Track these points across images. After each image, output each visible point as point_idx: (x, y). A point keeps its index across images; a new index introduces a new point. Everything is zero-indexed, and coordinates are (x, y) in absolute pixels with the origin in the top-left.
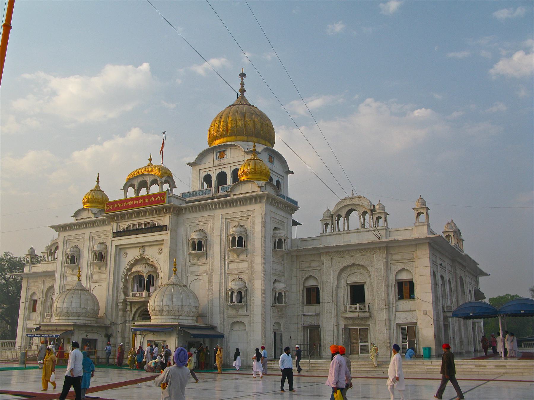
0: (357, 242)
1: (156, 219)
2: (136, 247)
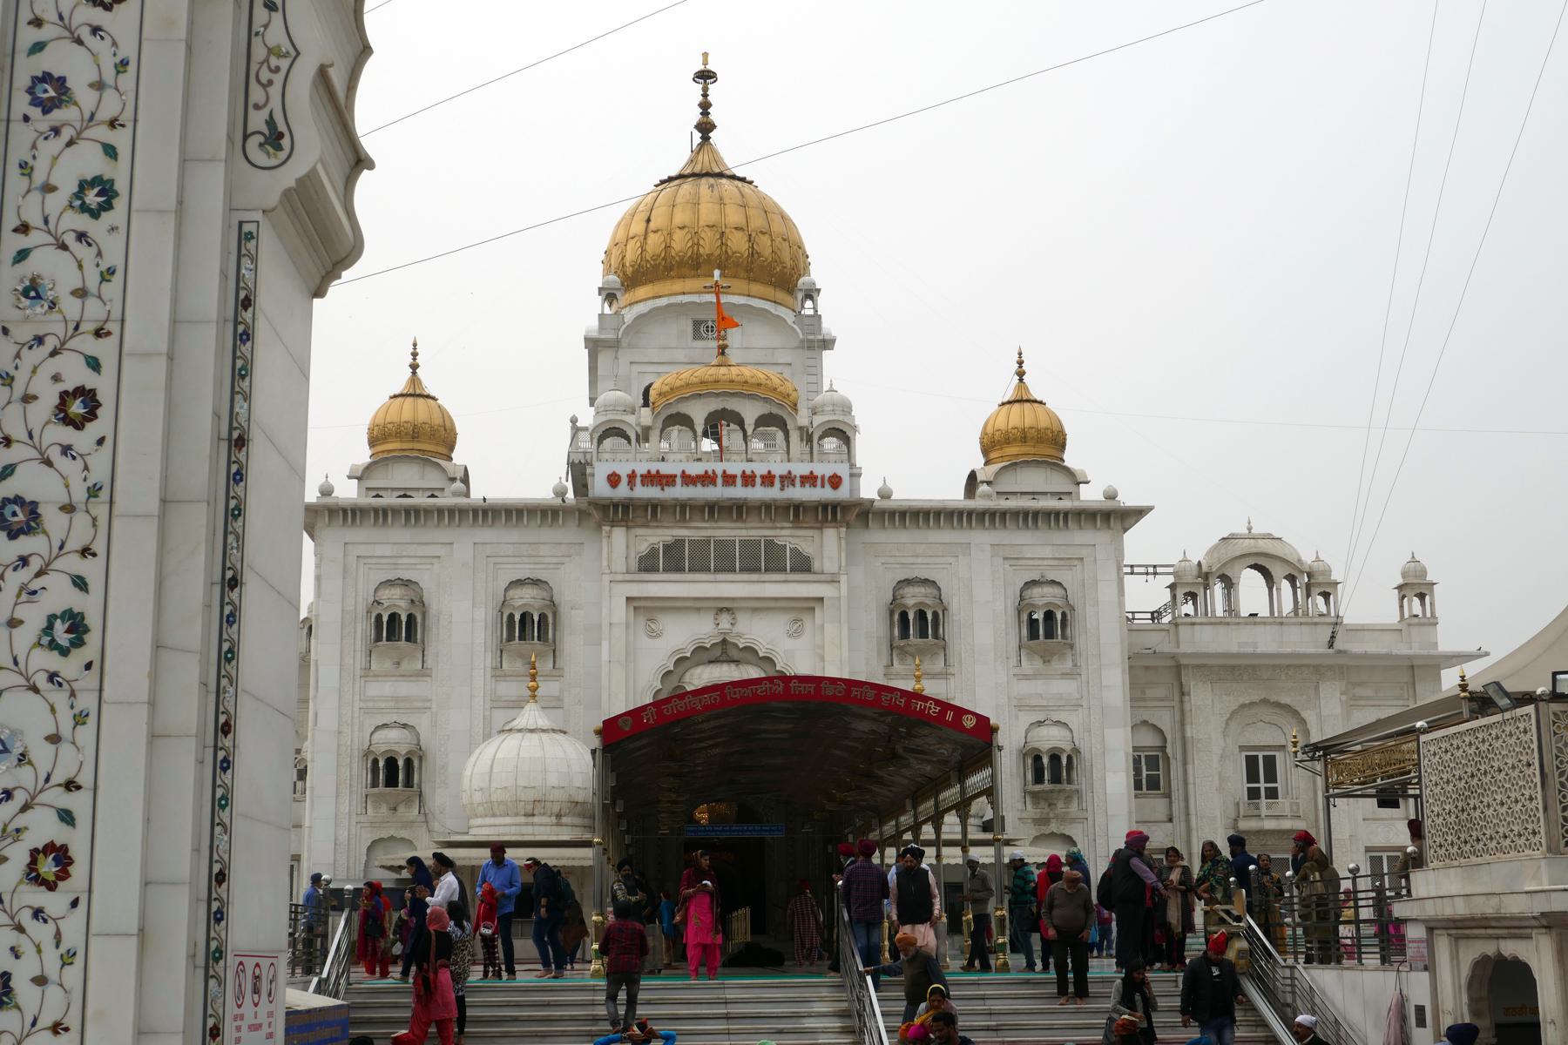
0: (1272, 648)
2: (699, 609)
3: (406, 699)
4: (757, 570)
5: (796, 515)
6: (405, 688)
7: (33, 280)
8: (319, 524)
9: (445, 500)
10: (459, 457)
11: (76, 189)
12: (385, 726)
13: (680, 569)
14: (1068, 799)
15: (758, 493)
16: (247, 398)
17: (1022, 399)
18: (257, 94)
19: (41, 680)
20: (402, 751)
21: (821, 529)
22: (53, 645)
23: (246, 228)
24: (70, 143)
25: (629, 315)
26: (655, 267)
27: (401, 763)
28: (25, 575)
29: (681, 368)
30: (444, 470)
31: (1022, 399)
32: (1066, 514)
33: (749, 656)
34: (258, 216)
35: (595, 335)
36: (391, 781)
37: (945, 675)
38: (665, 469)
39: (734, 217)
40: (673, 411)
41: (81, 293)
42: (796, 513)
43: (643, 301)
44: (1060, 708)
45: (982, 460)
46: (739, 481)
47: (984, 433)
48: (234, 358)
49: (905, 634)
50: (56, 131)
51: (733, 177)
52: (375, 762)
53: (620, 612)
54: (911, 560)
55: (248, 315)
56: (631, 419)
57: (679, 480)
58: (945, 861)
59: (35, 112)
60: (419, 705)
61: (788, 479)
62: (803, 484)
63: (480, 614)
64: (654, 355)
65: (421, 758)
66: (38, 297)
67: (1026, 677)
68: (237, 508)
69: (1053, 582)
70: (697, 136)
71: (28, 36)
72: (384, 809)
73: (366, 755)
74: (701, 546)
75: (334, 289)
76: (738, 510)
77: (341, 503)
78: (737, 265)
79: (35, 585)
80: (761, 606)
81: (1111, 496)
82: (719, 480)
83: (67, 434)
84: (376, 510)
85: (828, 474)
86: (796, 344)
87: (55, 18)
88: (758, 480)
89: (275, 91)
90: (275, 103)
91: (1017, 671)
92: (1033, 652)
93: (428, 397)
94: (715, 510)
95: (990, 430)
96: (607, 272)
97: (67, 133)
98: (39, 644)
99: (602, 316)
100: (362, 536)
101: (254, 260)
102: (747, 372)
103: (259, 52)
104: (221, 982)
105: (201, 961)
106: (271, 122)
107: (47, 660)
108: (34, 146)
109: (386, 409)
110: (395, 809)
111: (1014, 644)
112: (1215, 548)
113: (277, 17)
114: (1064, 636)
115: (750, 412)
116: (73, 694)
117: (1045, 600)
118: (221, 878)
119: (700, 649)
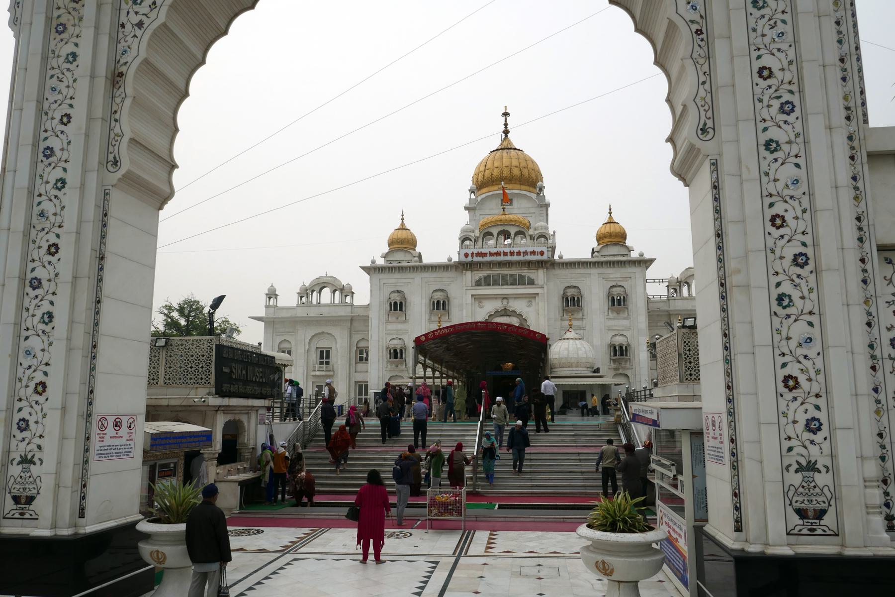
1: (525, 271)
2: (496, 298)
3: (400, 330)
4: (516, 284)
5: (529, 265)
6: (400, 326)
7: (42, 211)
8: (371, 273)
9: (412, 264)
10: (418, 249)
11: (55, 182)
12: (394, 339)
13: (489, 285)
14: (626, 362)
15: (515, 258)
16: (105, 245)
17: (611, 222)
18: (111, 149)
19: (40, 333)
20: (398, 347)
21: (537, 270)
22: (44, 322)
23: (107, 191)
24: (54, 168)
25: (479, 199)
26: (488, 181)
27: (398, 351)
28: (37, 301)
29: (489, 216)
30: (412, 254)
31: (611, 222)
32: (625, 262)
33: (513, 314)
34: (110, 187)
35: (468, 206)
36: (396, 357)
37: (582, 319)
38: (484, 251)
39: (515, 163)
40: (486, 231)
41: (55, 214)
42: (529, 264)
43: (485, 193)
44: (623, 330)
45: (597, 244)
46: (509, 254)
47: (597, 234)
48: (102, 232)
49: (567, 306)
50: (50, 164)
51: (515, 149)
52: (390, 350)
53: (469, 299)
54: (570, 280)
55: (106, 219)
56: (472, 234)
57: (488, 254)
58: (436, 384)
59: (44, 159)
60: (404, 332)
61: (525, 253)
62: (531, 254)
63: (424, 301)
64: (488, 212)
65: (405, 349)
66: (43, 216)
67: (610, 319)
68: (101, 279)
69: (620, 286)
70: (503, 136)
71: (43, 135)
72: (394, 366)
73: (388, 348)
74: (496, 277)
75: (166, 207)
76: (509, 264)
77: (378, 266)
78: (516, 179)
79: (39, 304)
80: (517, 297)
81: (641, 255)
82: (502, 254)
83: (50, 258)
84: (389, 268)
85: (540, 251)
86: (536, 206)
87: (51, 130)
88: (515, 254)
89: (116, 148)
90: (116, 151)
91: (607, 317)
92: (613, 311)
93: (407, 229)
94: (501, 264)
95: (599, 233)
96: (473, 184)
97: (53, 165)
98: (40, 322)
99: (470, 199)
100: (384, 276)
101: (108, 201)
102: (511, 217)
103: (112, 135)
104: (91, 423)
105: (85, 417)
106: (115, 158)
107: (42, 326)
108: (44, 170)
109: (393, 234)
110: (397, 366)
111: (606, 308)
112: (683, 272)
113: (118, 124)
114: (624, 305)
115: (513, 231)
116: (49, 337)
117: (617, 292)
118: (91, 392)
119: (497, 312)
